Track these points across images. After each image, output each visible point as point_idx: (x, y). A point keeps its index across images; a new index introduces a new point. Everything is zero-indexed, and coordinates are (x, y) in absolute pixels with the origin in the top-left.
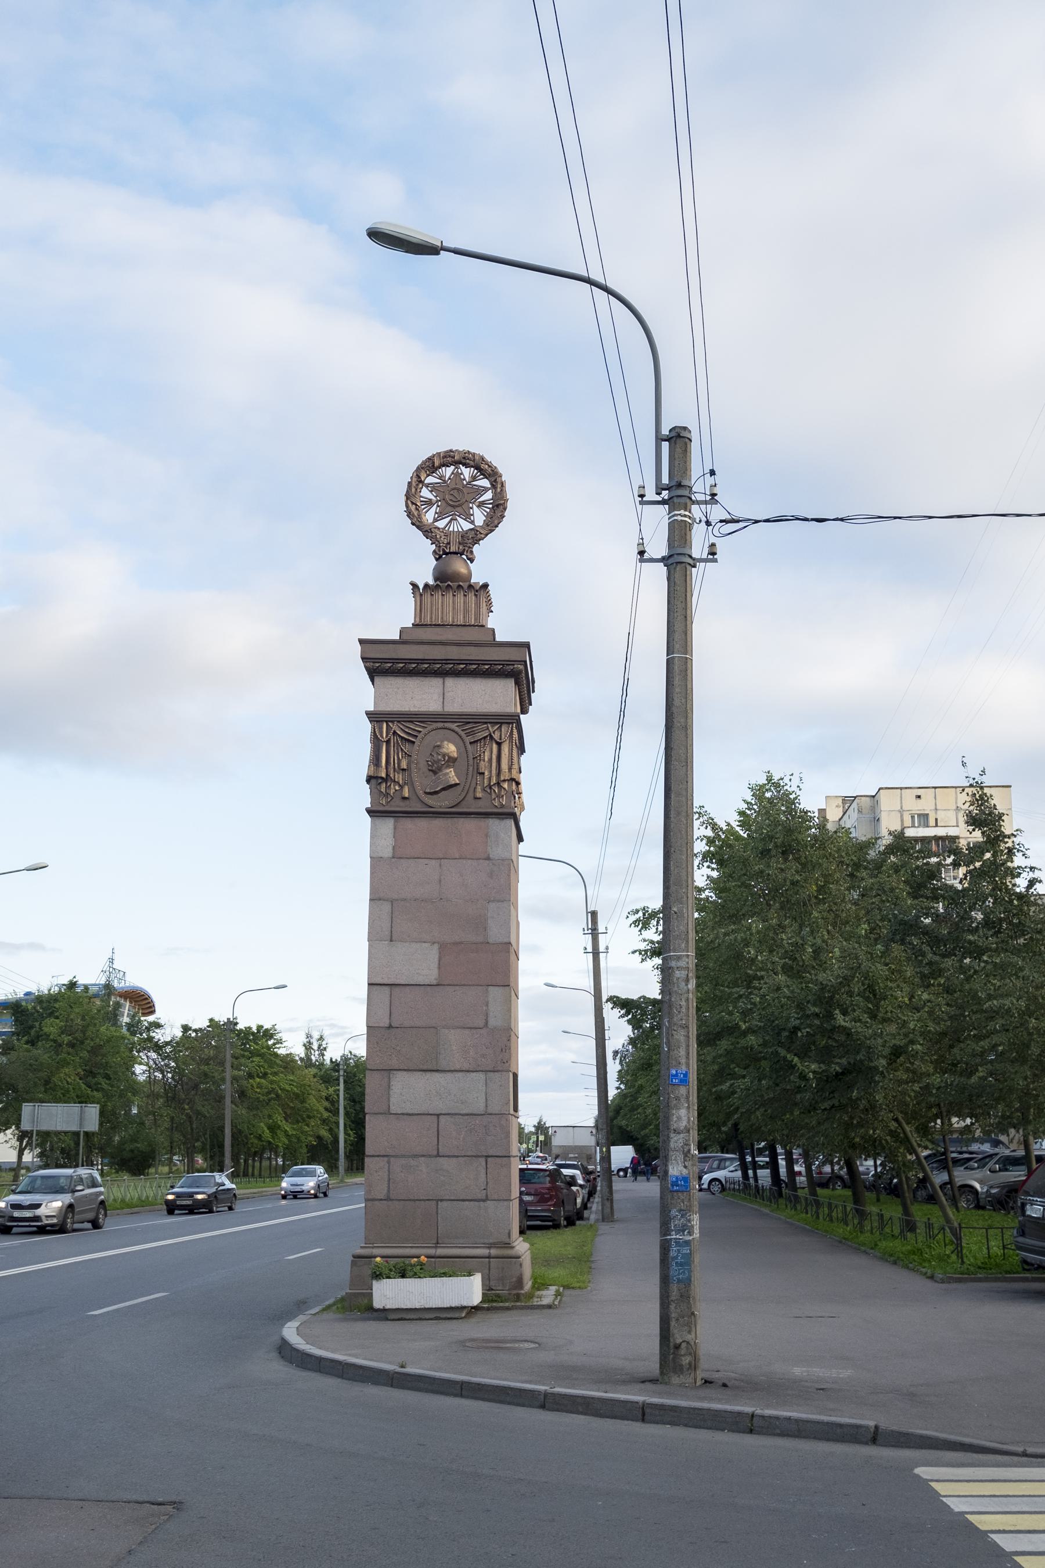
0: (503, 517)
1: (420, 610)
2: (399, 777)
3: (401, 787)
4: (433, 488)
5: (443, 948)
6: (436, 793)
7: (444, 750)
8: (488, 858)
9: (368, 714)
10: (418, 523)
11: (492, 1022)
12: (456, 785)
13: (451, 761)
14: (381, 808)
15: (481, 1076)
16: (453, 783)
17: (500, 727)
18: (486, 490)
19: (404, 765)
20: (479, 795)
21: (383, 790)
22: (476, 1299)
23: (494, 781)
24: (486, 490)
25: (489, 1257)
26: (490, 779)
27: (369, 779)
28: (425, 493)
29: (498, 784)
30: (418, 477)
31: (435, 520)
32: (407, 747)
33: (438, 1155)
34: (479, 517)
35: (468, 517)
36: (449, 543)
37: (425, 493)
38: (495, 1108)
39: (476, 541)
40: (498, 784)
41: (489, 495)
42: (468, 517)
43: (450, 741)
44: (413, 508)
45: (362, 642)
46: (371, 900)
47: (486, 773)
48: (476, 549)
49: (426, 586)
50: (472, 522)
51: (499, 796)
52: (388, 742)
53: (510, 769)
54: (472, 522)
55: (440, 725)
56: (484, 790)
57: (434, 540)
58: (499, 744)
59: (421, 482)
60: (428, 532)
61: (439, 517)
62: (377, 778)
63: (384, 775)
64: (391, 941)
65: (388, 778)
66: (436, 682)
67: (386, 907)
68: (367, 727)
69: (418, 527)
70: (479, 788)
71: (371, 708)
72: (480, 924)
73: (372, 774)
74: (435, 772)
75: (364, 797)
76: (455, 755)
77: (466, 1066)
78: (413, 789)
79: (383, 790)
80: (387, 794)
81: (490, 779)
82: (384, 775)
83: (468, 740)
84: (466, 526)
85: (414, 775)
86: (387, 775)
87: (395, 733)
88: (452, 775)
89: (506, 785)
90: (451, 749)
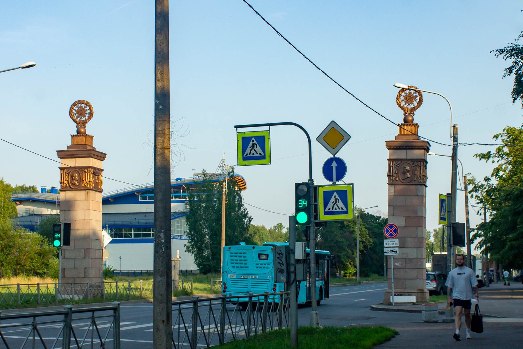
0: (422, 104)
1: (400, 131)
2: (395, 175)
3: (396, 178)
4: (404, 96)
5: (407, 218)
6: (404, 179)
7: (407, 169)
8: (417, 195)
9: (387, 159)
10: (399, 106)
11: (418, 236)
12: (409, 177)
13: (408, 171)
14: (391, 183)
15: (415, 249)
16: (409, 177)
17: (420, 163)
18: (417, 96)
19: (397, 172)
20: (415, 180)
21: (391, 178)
22: (414, 301)
23: (419, 176)
24: (417, 96)
25: (418, 292)
26: (418, 175)
27: (388, 176)
28: (401, 97)
29: (420, 177)
30: (400, 93)
31: (404, 105)
32: (397, 168)
33: (405, 268)
34: (416, 104)
35: (413, 104)
36: (408, 111)
37: (401, 97)
38: (419, 257)
39: (415, 110)
40: (420, 177)
41: (418, 98)
42: (413, 104)
43: (408, 166)
44: (398, 102)
45: (386, 141)
46: (389, 206)
47: (417, 174)
48: (415, 112)
49: (402, 124)
50: (414, 105)
51: (420, 180)
52: (393, 166)
53: (423, 173)
54: (414, 105)
55: (406, 162)
56: (416, 178)
57: (404, 111)
58: (420, 167)
59: (401, 95)
60: (402, 108)
61: (406, 103)
62: (390, 175)
63: (391, 175)
64: (393, 216)
65: (392, 176)
66: (404, 151)
67: (392, 208)
68: (387, 162)
69: (400, 107)
70: (415, 178)
71: (388, 158)
72: (415, 212)
73: (388, 174)
74: (404, 174)
75: (386, 180)
76: (409, 170)
77: (412, 247)
78: (399, 178)
79: (391, 178)
80: (393, 180)
81: (418, 175)
82: (391, 175)
83: (413, 166)
84: (412, 106)
85: (399, 175)
86: (392, 175)
87: (394, 164)
88: (408, 175)
89: (422, 177)
90: (408, 168)
